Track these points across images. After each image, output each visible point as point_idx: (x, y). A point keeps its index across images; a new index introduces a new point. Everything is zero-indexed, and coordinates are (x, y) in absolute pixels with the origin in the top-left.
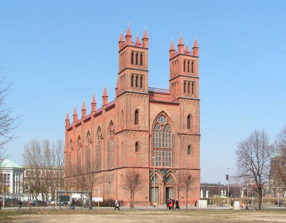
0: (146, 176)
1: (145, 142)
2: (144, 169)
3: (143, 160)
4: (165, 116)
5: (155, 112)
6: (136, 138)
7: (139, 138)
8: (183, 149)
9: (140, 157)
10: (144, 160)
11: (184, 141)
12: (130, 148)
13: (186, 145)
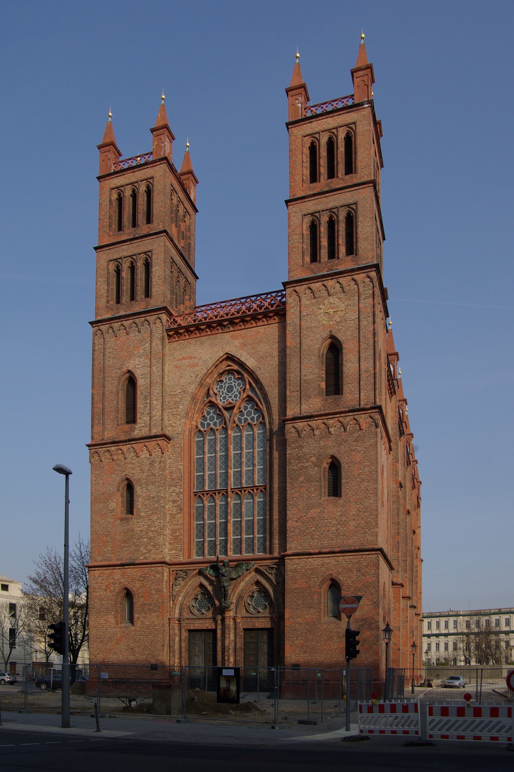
1: (149, 476)
2: (146, 569)
3: (141, 537)
4: (238, 373)
5: (197, 365)
6: (120, 468)
7: (130, 466)
8: (302, 479)
9: (133, 530)
10: (145, 540)
11: (301, 447)
12: (101, 505)
13: (313, 459)
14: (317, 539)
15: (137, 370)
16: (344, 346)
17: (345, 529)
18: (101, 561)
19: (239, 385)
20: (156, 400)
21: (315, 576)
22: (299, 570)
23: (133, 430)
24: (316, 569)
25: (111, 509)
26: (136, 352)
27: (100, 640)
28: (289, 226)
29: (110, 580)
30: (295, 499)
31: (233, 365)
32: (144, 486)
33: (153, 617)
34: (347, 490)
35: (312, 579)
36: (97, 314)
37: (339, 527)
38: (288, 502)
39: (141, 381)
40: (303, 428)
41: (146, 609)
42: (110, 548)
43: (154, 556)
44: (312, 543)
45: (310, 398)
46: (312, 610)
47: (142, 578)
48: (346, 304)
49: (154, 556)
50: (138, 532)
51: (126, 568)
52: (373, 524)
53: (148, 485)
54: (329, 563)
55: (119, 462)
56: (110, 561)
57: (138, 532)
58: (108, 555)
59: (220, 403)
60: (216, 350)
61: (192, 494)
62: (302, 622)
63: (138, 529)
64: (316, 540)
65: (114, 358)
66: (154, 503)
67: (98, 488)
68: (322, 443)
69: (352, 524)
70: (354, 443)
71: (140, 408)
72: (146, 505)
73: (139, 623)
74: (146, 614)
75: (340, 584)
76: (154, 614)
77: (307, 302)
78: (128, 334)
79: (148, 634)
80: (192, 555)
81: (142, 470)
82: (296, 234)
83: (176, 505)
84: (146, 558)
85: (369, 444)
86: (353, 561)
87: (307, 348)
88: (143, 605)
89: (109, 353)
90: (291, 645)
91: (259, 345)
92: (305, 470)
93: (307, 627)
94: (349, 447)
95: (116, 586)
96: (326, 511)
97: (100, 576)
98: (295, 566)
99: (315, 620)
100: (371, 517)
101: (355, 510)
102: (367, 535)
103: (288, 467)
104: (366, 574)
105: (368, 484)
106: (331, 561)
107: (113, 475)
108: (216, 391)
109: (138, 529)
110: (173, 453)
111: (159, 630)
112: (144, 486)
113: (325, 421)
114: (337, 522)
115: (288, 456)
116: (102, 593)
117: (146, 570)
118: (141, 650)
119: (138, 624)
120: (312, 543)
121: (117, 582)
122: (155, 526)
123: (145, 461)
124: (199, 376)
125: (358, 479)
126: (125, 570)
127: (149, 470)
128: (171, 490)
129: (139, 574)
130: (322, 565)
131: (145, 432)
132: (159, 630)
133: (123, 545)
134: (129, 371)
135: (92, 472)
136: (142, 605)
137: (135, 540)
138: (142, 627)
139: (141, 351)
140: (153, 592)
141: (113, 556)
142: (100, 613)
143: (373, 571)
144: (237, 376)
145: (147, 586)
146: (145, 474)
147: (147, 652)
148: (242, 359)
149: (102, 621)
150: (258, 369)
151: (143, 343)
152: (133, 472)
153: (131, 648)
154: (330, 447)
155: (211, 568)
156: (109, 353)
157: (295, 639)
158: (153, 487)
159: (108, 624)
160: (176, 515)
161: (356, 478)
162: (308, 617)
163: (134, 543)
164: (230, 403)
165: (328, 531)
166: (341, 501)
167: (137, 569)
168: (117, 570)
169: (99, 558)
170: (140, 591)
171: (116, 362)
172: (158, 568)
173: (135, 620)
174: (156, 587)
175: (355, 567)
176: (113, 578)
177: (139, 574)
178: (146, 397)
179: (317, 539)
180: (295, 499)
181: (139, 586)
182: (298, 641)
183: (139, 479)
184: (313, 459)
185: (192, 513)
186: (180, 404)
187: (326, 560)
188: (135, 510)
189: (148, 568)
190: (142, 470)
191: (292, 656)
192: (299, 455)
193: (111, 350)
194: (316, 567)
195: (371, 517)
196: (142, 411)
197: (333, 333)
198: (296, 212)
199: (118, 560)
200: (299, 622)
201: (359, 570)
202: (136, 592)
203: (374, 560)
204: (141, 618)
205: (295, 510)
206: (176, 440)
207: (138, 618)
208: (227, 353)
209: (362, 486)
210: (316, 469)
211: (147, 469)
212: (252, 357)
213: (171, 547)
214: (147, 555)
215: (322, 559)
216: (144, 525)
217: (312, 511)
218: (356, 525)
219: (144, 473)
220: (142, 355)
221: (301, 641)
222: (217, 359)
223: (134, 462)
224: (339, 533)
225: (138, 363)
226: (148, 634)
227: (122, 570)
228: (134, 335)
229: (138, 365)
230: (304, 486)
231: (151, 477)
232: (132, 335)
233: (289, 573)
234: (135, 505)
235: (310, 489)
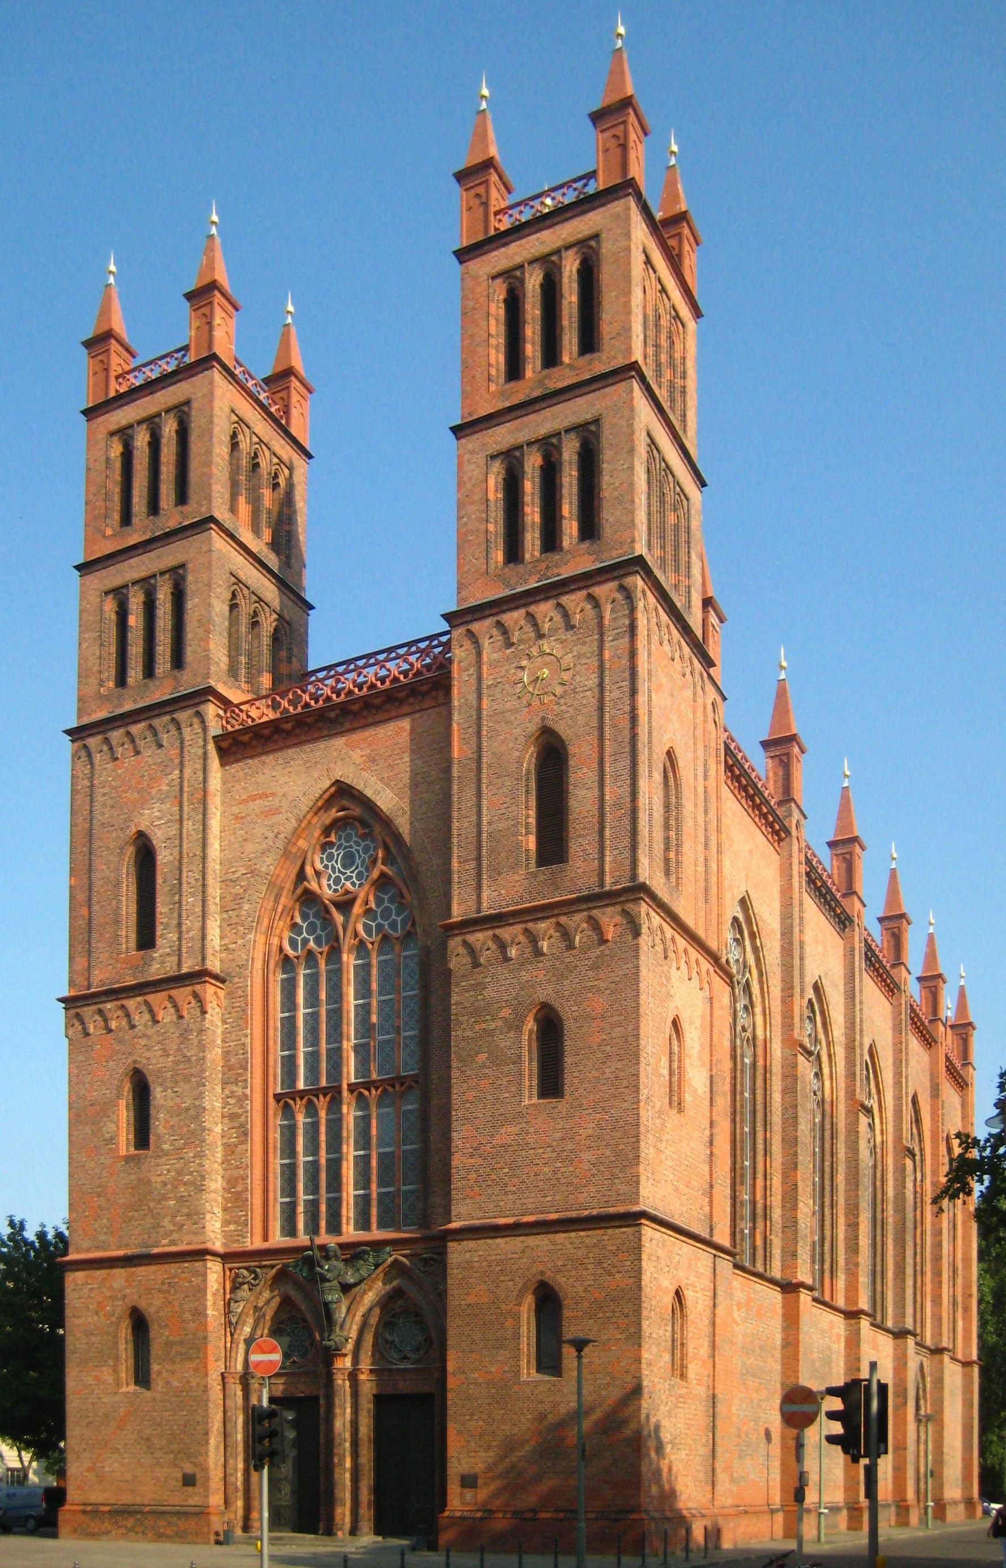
0: (187, 1316)
2: (173, 1268)
3: (164, 1198)
5: (277, 811)
8: (482, 1057)
9: (149, 1181)
10: (172, 1202)
11: (480, 986)
12: (88, 1129)
13: (506, 1012)
14: (514, 1193)
15: (156, 831)
16: (572, 749)
17: (571, 1169)
18: (89, 1250)
19: (366, 849)
20: (193, 895)
22: (475, 1264)
23: (147, 963)
24: (510, 1262)
25: (107, 1136)
26: (154, 792)
27: (87, 1421)
28: (460, 485)
29: (104, 1290)
30: (468, 1105)
31: (352, 806)
32: (169, 1085)
34: (575, 1080)
35: (503, 1285)
36: (81, 713)
37: (560, 1165)
38: (453, 1113)
39: (164, 853)
40: (484, 943)
41: (173, 1353)
42: (105, 1221)
43: (189, 1238)
44: (502, 1204)
45: (500, 874)
46: (502, 1352)
47: (165, 1287)
48: (575, 653)
49: (189, 1238)
50: (159, 1186)
52: (631, 1156)
53: (176, 1082)
55: (121, 1034)
56: (105, 1250)
57: (159, 1186)
58: (102, 1237)
59: (327, 891)
60: (316, 775)
61: (271, 1100)
62: (481, 1380)
63: (159, 1179)
64: (511, 1197)
65: (112, 807)
66: (188, 1122)
67: (82, 1092)
68: (525, 976)
69: (587, 1156)
70: (590, 973)
71: (161, 913)
72: (172, 1126)
73: (161, 1384)
74: (173, 1363)
75: (561, 1294)
76: (189, 1365)
77: (495, 656)
78: (138, 753)
80: (270, 1233)
81: (165, 1050)
82: (473, 502)
83: (236, 1124)
84: (173, 1242)
85: (621, 973)
86: (587, 1241)
87: (494, 760)
88: (169, 1344)
89: (104, 795)
91: (401, 759)
92: (489, 1039)
93: (493, 1391)
94: (581, 981)
96: (532, 1130)
97: (87, 1283)
98: (468, 1255)
100: (625, 1140)
101: (592, 1125)
102: (617, 1181)
103: (453, 1033)
104: (614, 1270)
105: (619, 1065)
106: (539, 1242)
107: (111, 1063)
108: (319, 866)
109: (159, 1179)
110: (229, 1010)
112: (169, 1085)
113: (530, 925)
114: (554, 1155)
115: (454, 1007)
116: (90, 1319)
119: (158, 1385)
120: (502, 1204)
121: (119, 1296)
122: (191, 1173)
123: (172, 1031)
124: (282, 836)
125: (599, 1055)
126: (133, 1269)
127: (179, 1050)
128: (227, 1092)
130: (523, 1252)
131: (170, 968)
133: (130, 1214)
134: (141, 835)
135: (70, 1058)
137: (152, 1205)
138: (167, 1393)
139: (165, 788)
140: (187, 1316)
141: (111, 1239)
142: (86, 1362)
143: (629, 1263)
144: (361, 831)
145: (176, 1303)
146: (171, 1058)
148: (369, 793)
149: (91, 1381)
150: (400, 813)
151: (168, 770)
152: (148, 1054)
154: (540, 984)
155: (304, 1263)
156: (104, 795)
157: (467, 1417)
158: (187, 1086)
159: (102, 1387)
160: (236, 1146)
161: (593, 1053)
162: (493, 1370)
163: (150, 1210)
164: (347, 892)
165: (536, 1175)
166: (562, 1106)
169: (85, 1245)
171: (115, 814)
173: (153, 1376)
174: (192, 1305)
175: (591, 1255)
176: (111, 1287)
177: (160, 1277)
178: (171, 893)
179: (514, 1193)
180: (468, 1105)
182: (474, 1423)
183: (159, 1070)
184: (506, 1012)
185: (271, 1141)
186: (245, 900)
187: (532, 1241)
188: (152, 1138)
190: (165, 1050)
192: (476, 1004)
193: (106, 790)
194: (510, 1256)
195: (625, 1140)
196: (165, 920)
197: (550, 723)
198: (473, 452)
199: (119, 1247)
200: (477, 1379)
201: (600, 1263)
202: (155, 1317)
203: (631, 1238)
204: (164, 1374)
205: (468, 1131)
206: (236, 980)
207: (159, 1373)
208: (337, 781)
209: (608, 1071)
210: (512, 1034)
211: (175, 1047)
212: (388, 785)
213: (228, 1217)
214: (176, 1236)
215: (521, 1238)
216: (169, 1171)
217: (503, 1131)
218: (593, 1159)
219: (168, 1055)
220: (167, 797)
221: (481, 1423)
222: (317, 795)
223: (150, 1032)
224: (558, 1179)
225: (157, 814)
228: (149, 754)
229: (160, 818)
230: (486, 1076)
231: (182, 1066)
232: (147, 753)
234: (152, 1126)
235: (499, 1082)
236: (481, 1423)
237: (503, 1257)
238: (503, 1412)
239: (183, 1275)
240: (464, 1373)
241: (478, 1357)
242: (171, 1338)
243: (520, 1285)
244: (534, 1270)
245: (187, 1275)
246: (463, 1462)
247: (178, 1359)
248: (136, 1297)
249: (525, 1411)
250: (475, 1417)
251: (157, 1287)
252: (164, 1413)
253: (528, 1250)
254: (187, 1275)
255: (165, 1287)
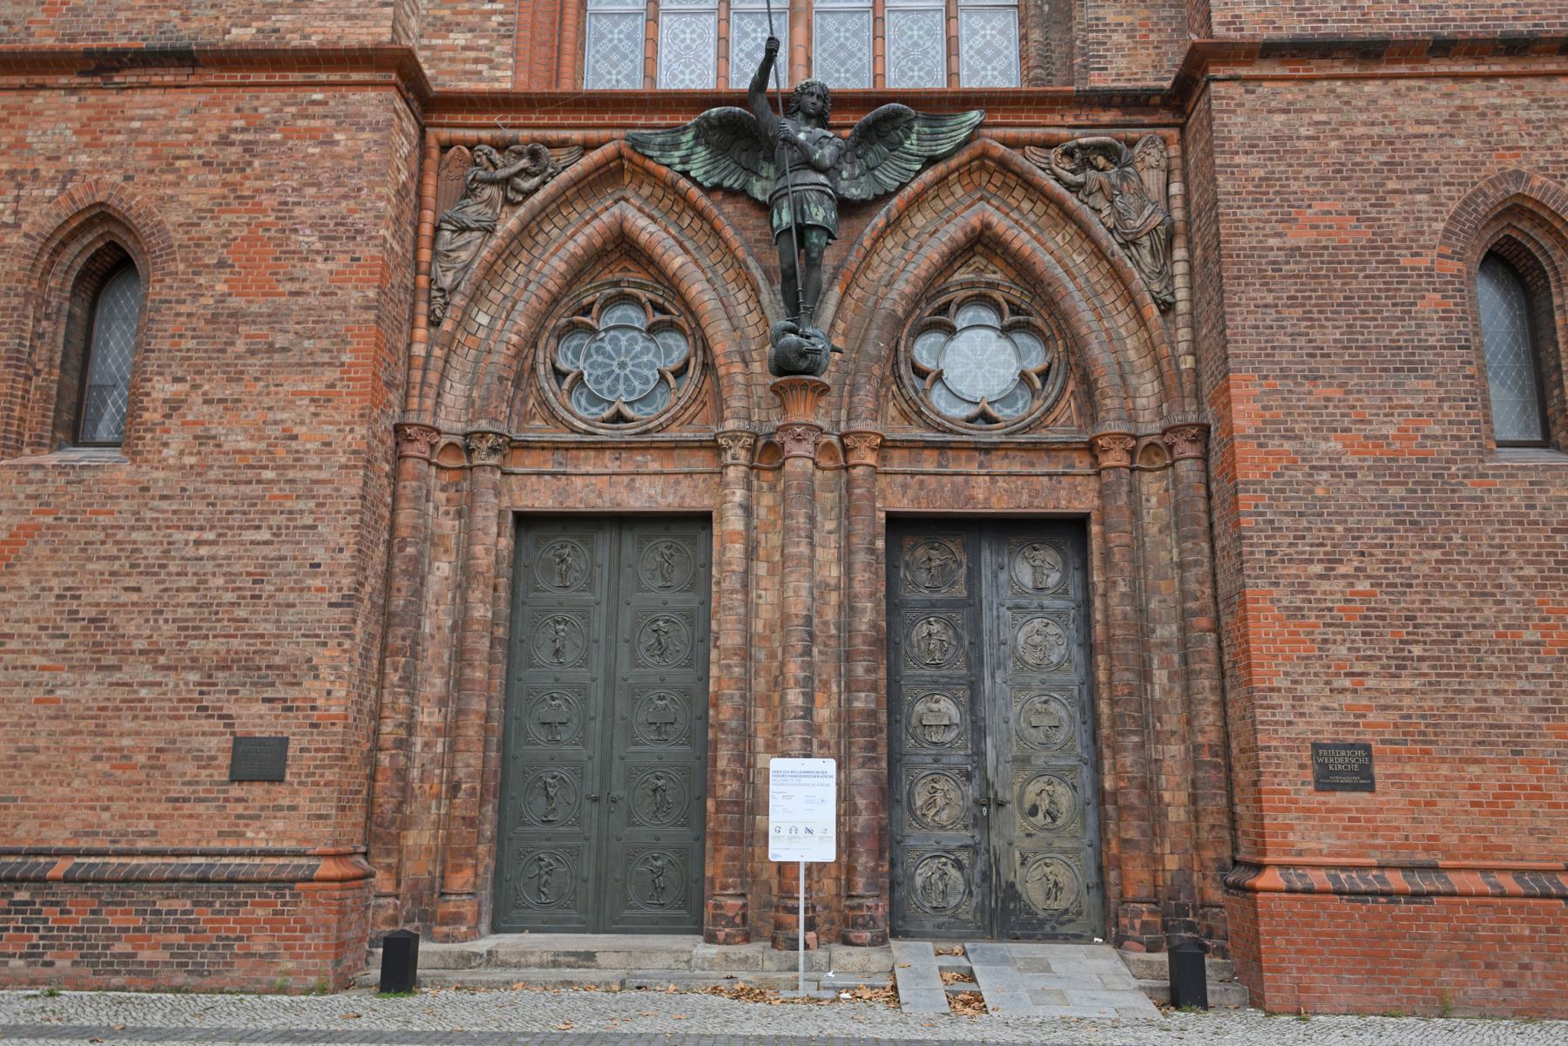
21: (1413, 185)
22: (1301, 144)
24: (1423, 143)
33: (289, 404)
35: (1398, 202)
46: (1412, 383)
47: (233, 153)
51: (121, 88)
54: (1497, 110)
62: (1350, 460)
74: (236, 378)
79: (236, 520)
90: (1295, 613)
93: (1396, 492)
95: (32, 191)
99: (1446, 448)
111: (322, 490)
117: (268, 103)
118: (168, 629)
126: (112, 98)
129: (213, 125)
130: (1453, 119)
132: (322, 490)
136: (213, 319)
138: (200, 471)
141: (42, 16)
145: (267, 201)
147: (212, 644)
153: (86, 612)
157: (1318, 569)
162: (1390, 431)
167: (202, 97)
168: (60, 98)
170: (208, 227)
172: (355, 97)
181: (203, 202)
182: (1338, 585)
189: (283, 95)
191: (1306, 689)
194: (1411, 129)
202: (178, 237)
204: (196, 409)
207: (174, 406)
226: (236, 520)
227: (92, 98)
233: (1240, 159)
236: (1363, 585)
237: (1391, 130)
238: (1437, 554)
239: (302, 123)
240: (1290, 436)
241: (1337, 394)
242: (236, 302)
243: (1453, 206)
244: (1492, 167)
245: (317, 123)
246: (1312, 707)
247: (255, 365)
248: (116, 177)
249: (1513, 555)
250: (1341, 569)
251: (201, 151)
252: (178, 536)
253: (1471, 119)
254: (317, 123)
255: (233, 153)
